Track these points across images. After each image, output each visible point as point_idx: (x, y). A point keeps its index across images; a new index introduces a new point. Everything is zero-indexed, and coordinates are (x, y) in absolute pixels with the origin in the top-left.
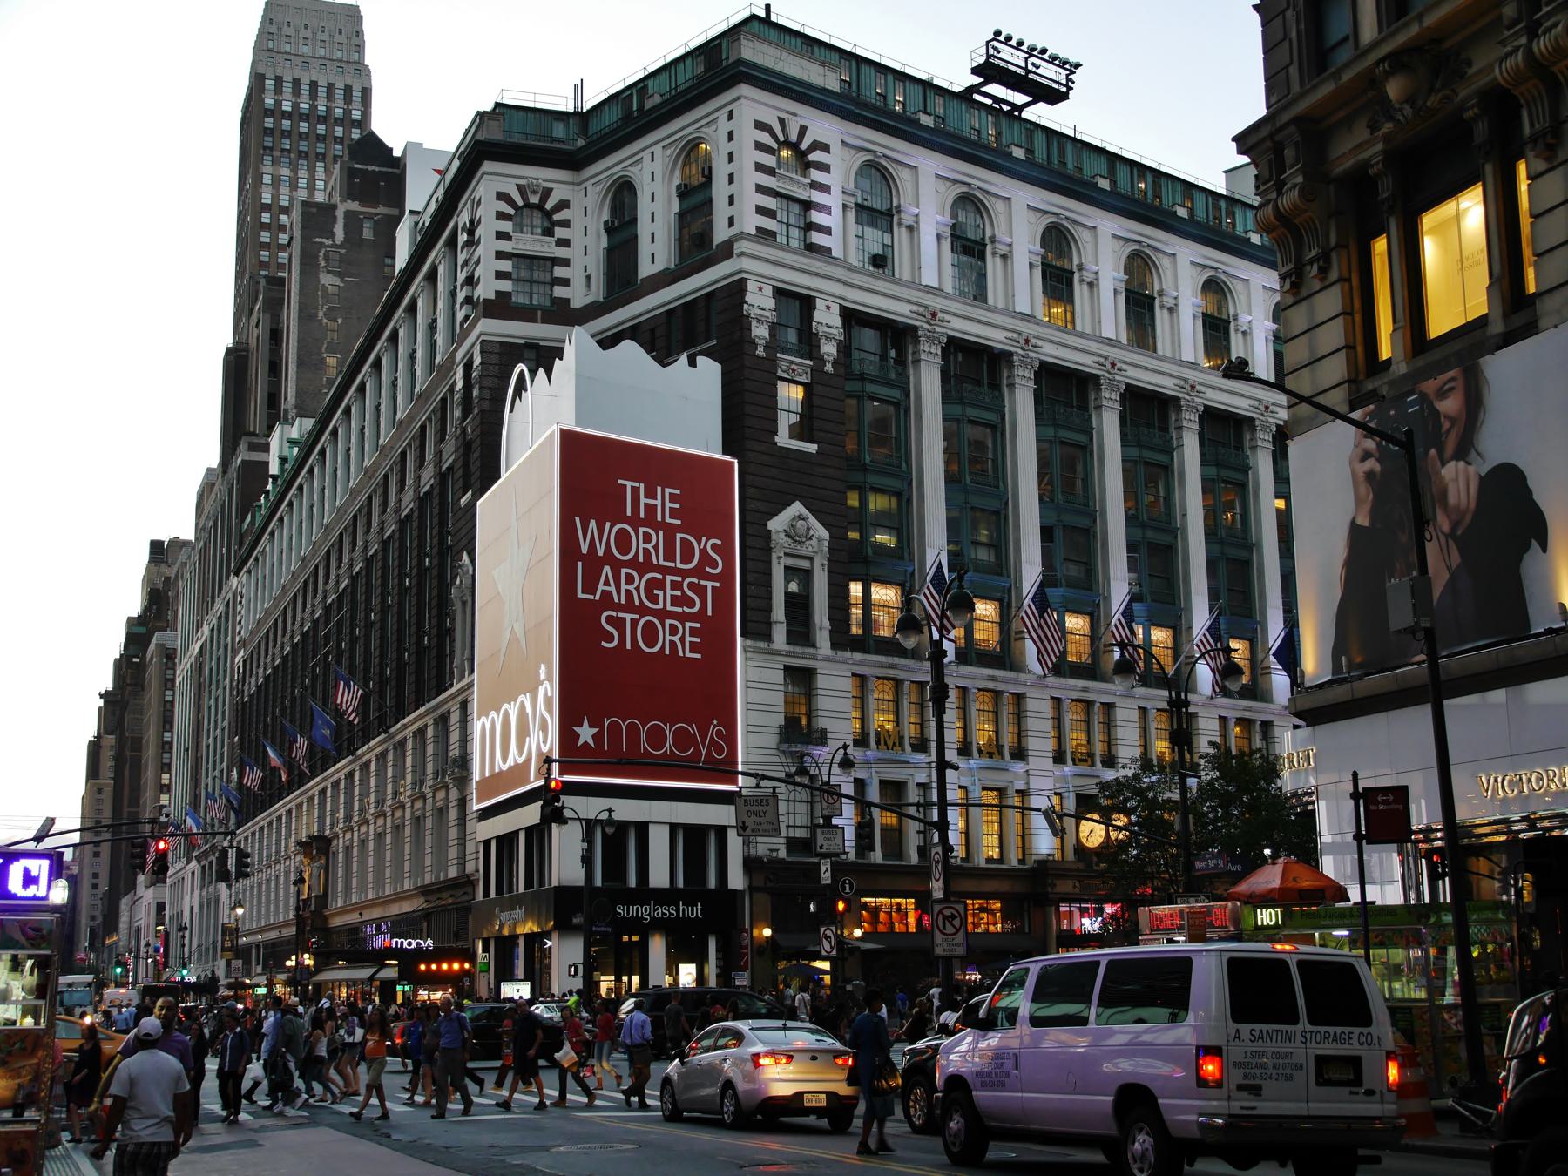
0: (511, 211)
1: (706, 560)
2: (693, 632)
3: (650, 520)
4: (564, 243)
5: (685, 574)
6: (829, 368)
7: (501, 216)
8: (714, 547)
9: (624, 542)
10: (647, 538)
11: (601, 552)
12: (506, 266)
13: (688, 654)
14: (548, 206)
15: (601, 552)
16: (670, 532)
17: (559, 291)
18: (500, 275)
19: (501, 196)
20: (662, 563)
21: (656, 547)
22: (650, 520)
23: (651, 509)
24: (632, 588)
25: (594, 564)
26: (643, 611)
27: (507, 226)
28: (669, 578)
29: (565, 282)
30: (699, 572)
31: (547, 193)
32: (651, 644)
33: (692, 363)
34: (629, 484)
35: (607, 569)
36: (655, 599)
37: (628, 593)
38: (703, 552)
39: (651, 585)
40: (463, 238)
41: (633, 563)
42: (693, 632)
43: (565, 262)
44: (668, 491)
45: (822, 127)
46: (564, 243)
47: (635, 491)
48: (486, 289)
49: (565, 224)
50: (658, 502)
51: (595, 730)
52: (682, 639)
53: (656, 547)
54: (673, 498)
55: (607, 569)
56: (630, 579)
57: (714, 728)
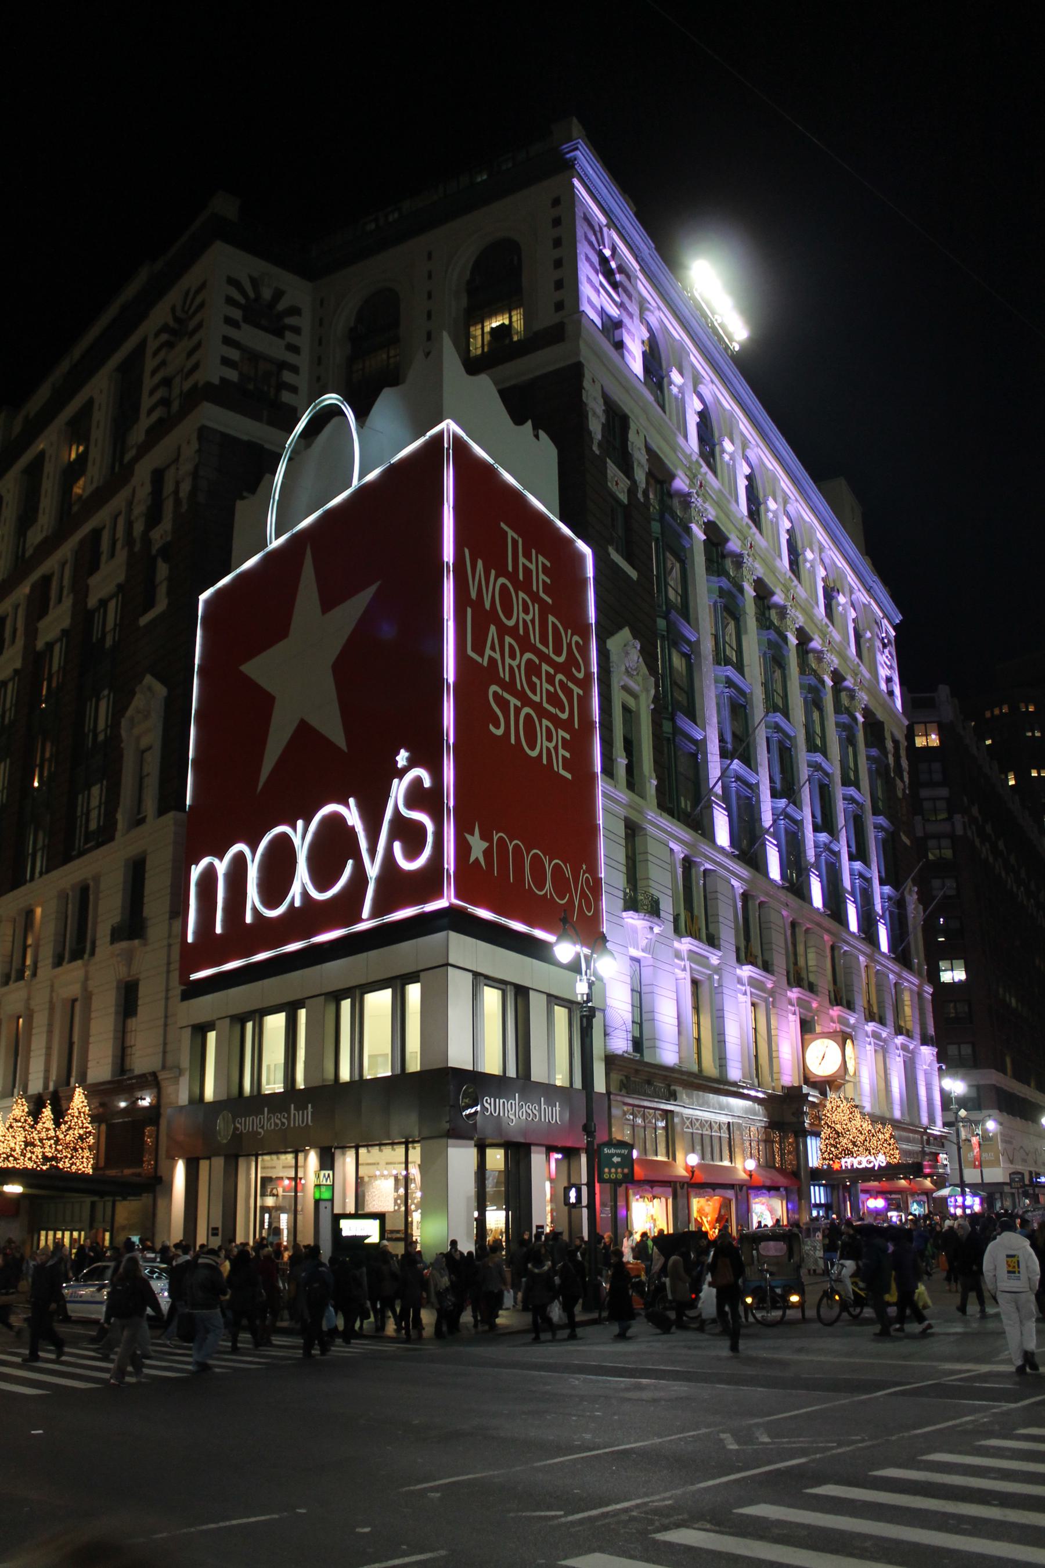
0: (243, 301)
3: (525, 585)
4: (294, 349)
5: (558, 668)
6: (640, 496)
7: (230, 301)
8: (577, 643)
10: (526, 611)
11: (488, 606)
12: (234, 355)
13: (562, 772)
14: (281, 306)
15: (488, 606)
17: (286, 397)
18: (226, 362)
19: (232, 281)
21: (533, 621)
22: (525, 585)
23: (527, 571)
24: (515, 664)
27: (237, 314)
28: (545, 667)
29: (294, 390)
31: (279, 294)
32: (532, 747)
34: (511, 533)
35: (493, 629)
36: (533, 687)
37: (511, 667)
38: (569, 645)
39: (532, 669)
40: (152, 345)
41: (513, 632)
43: (295, 369)
44: (541, 558)
46: (294, 349)
47: (515, 543)
48: (213, 372)
49: (297, 330)
51: (485, 845)
52: (556, 748)
53: (533, 621)
55: (493, 629)
56: (513, 656)
57: (584, 876)
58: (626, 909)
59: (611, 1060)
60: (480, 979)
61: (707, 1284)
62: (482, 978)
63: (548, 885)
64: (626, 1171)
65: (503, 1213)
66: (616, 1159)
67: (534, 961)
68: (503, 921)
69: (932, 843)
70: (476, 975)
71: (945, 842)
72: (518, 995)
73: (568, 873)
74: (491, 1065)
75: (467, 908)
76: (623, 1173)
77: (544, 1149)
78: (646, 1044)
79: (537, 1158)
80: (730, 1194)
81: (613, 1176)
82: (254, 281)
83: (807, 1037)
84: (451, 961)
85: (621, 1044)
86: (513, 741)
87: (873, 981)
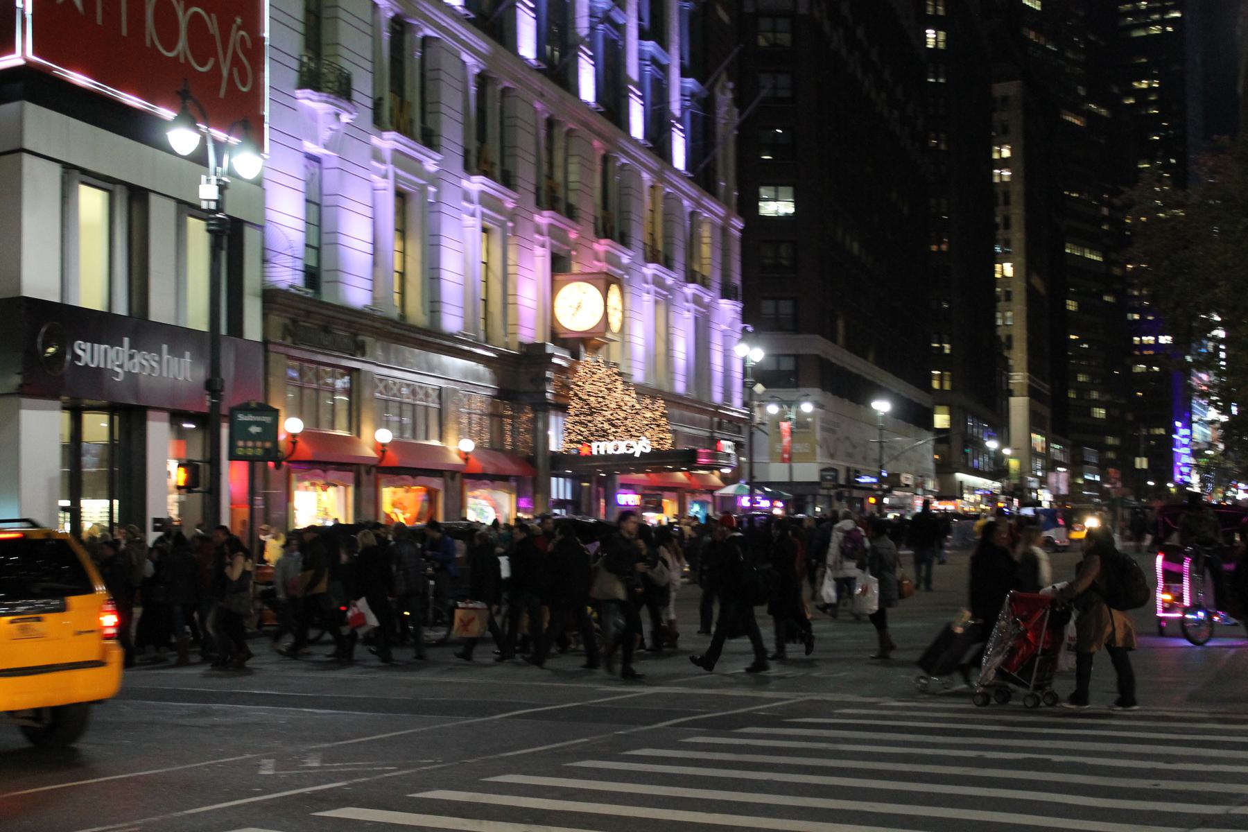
57: (238, 34)
58: (302, 86)
59: (271, 297)
60: (74, 175)
61: (383, 595)
62: (77, 173)
63: (182, 44)
64: (268, 445)
65: (107, 502)
66: (254, 429)
67: (148, 147)
68: (109, 91)
69: (765, 23)
70: (67, 167)
71: (783, 23)
72: (132, 201)
73: (213, 26)
74: (91, 293)
75: (51, 69)
76: (262, 448)
77: (166, 415)
78: (325, 276)
79: (158, 431)
80: (436, 483)
81: (250, 452)
83: (559, 278)
84: (28, 145)
85: (287, 275)
87: (660, 207)
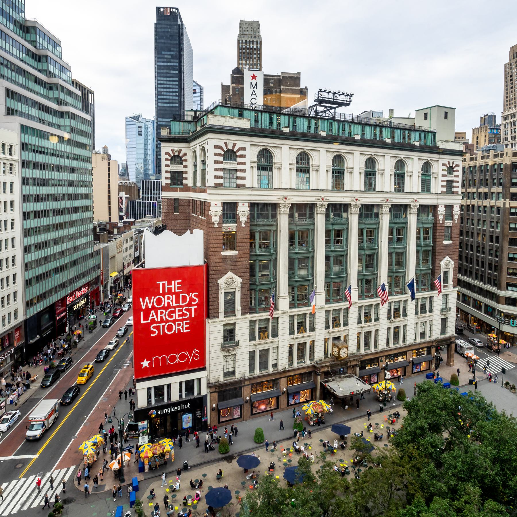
1: (191, 300)
2: (186, 324)
4: (186, 166)
8: (195, 296)
9: (159, 301)
11: (150, 307)
12: (169, 175)
13: (185, 331)
15: (150, 307)
16: (177, 295)
20: (174, 305)
21: (172, 301)
22: (170, 292)
23: (170, 290)
25: (147, 312)
26: (167, 321)
28: (177, 309)
29: (186, 179)
30: (189, 304)
31: (180, 151)
33: (192, 232)
34: (161, 283)
35: (153, 312)
36: (172, 317)
38: (191, 299)
41: (163, 308)
42: (186, 324)
44: (176, 281)
45: (241, 142)
46: (186, 166)
47: (164, 285)
49: (186, 160)
50: (173, 286)
52: (182, 327)
54: (178, 283)
55: (153, 312)
56: (162, 313)
57: (195, 351)
82: (172, 150)
86: (161, 334)
